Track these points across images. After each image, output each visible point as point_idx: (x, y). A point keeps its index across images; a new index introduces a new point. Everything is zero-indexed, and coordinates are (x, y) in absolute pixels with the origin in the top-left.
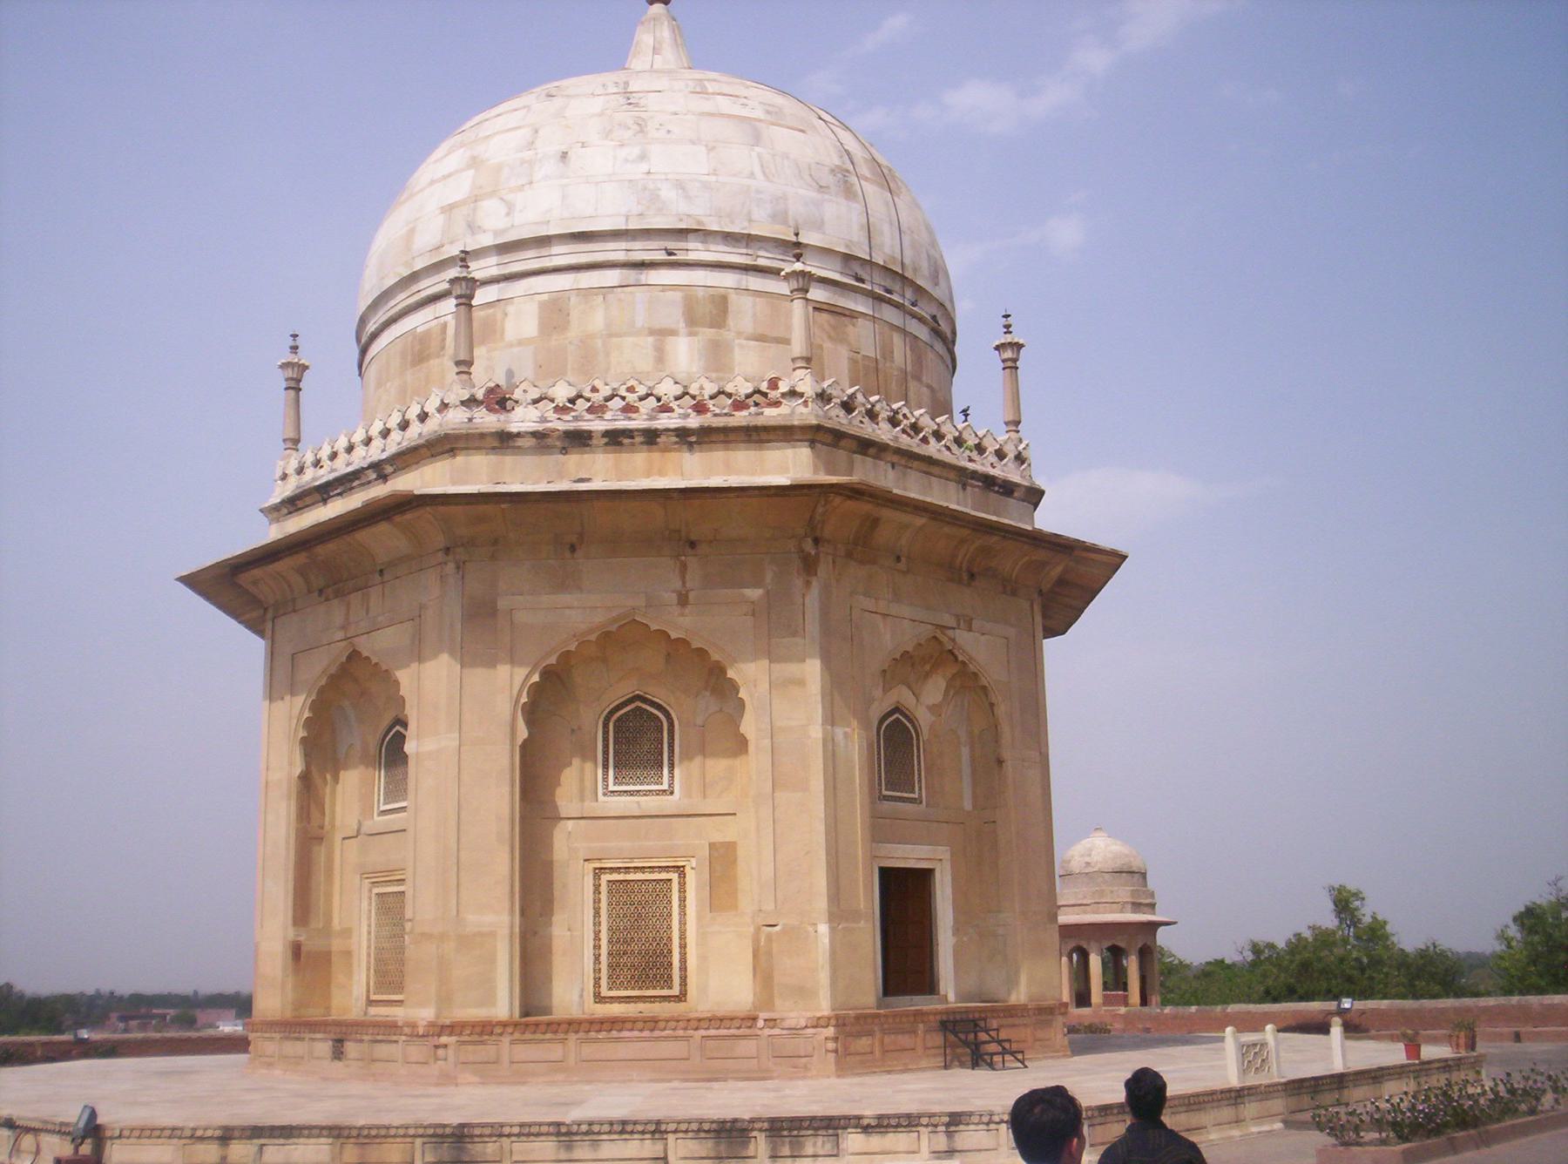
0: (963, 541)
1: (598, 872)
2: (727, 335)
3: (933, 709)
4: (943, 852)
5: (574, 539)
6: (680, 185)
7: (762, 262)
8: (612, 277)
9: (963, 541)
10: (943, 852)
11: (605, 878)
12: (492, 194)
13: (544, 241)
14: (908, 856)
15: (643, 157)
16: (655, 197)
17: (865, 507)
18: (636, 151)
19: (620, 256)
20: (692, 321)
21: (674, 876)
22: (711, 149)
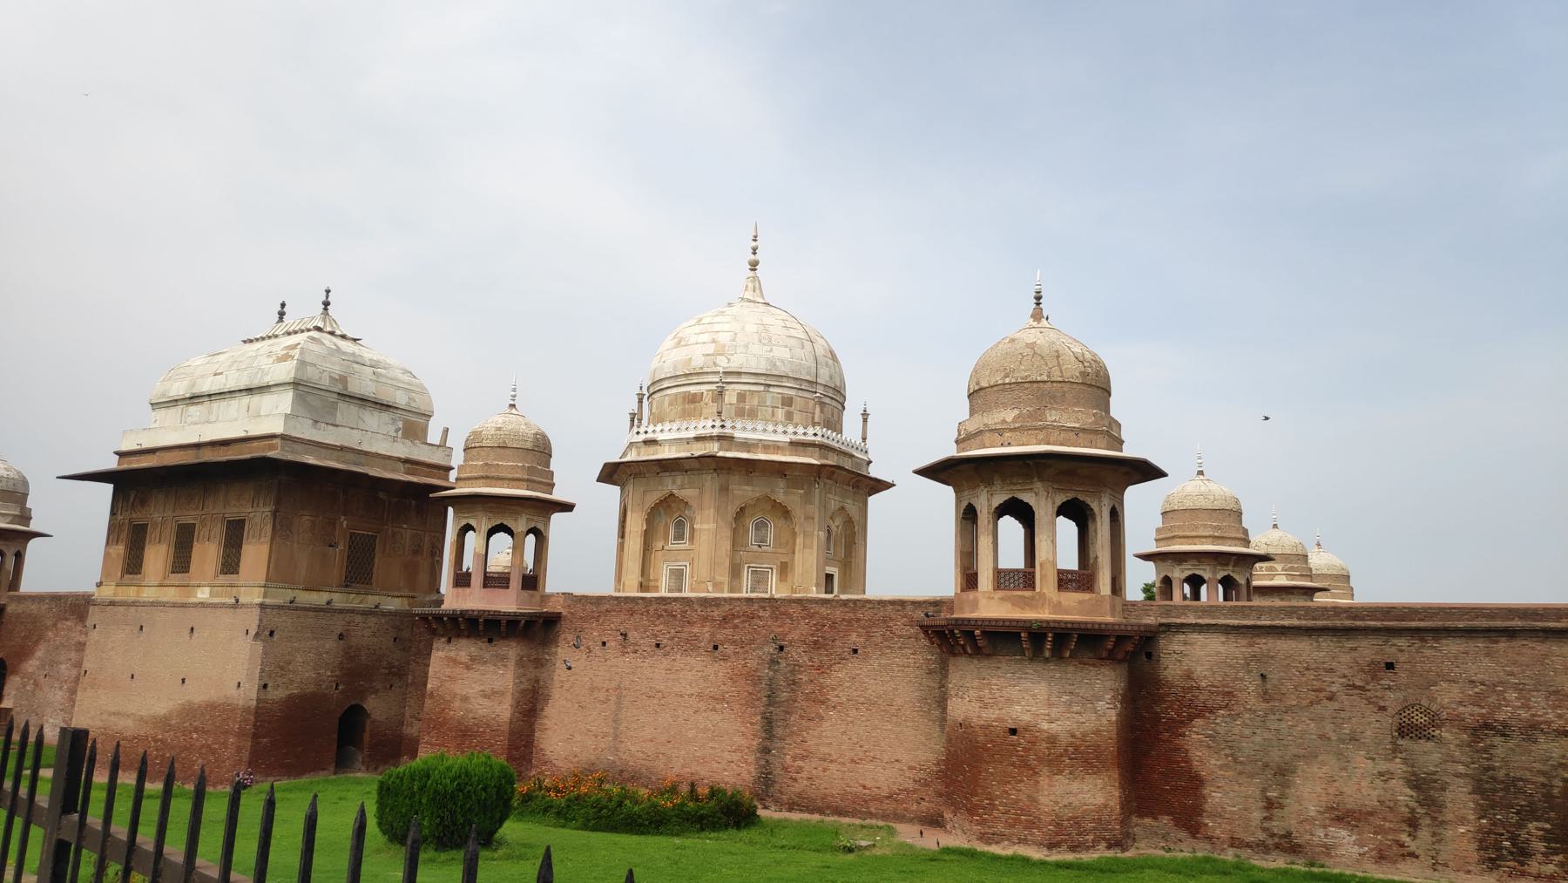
0: (853, 478)
1: (749, 567)
2: (792, 409)
3: (837, 527)
4: (836, 570)
5: (751, 470)
6: (782, 361)
7: (803, 387)
8: (762, 388)
9: (853, 478)
10: (836, 570)
11: (750, 569)
12: (722, 355)
13: (739, 374)
14: (830, 570)
15: (771, 350)
16: (775, 365)
17: (834, 469)
18: (769, 349)
19: (763, 382)
20: (782, 405)
21: (770, 570)
22: (790, 350)
